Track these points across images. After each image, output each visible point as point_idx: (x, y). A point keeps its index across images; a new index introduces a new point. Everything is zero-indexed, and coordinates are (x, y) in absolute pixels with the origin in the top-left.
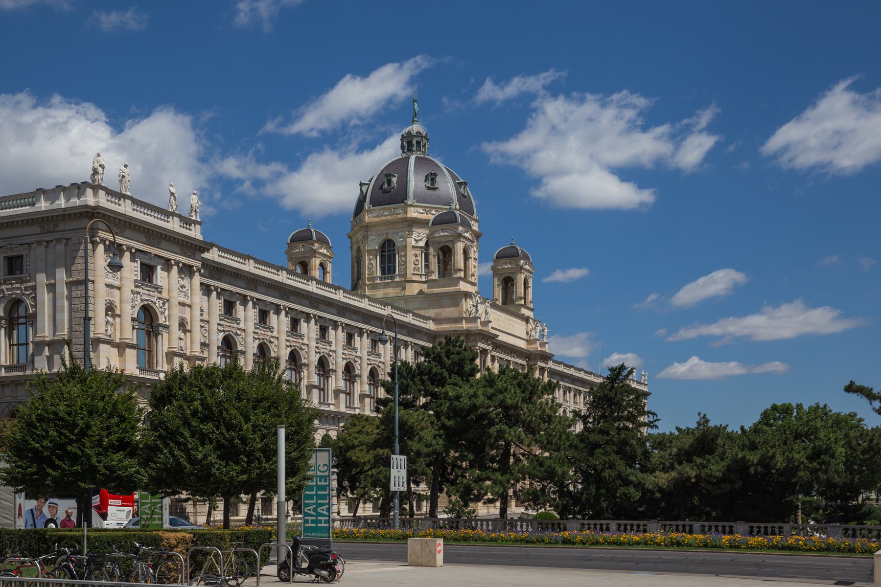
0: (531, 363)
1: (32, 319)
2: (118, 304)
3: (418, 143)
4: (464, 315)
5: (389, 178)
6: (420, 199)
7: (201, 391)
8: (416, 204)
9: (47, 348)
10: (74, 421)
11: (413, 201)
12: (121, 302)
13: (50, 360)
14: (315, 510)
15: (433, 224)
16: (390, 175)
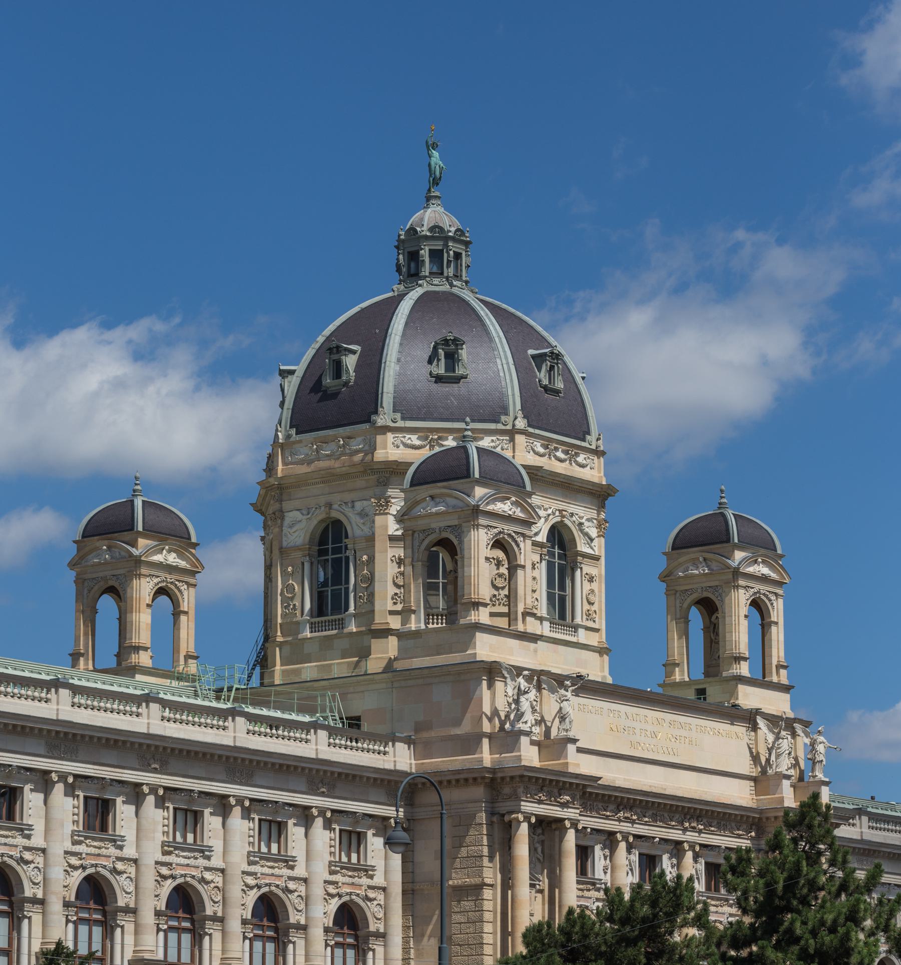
3: (436, 255)
5: (335, 357)
8: (401, 424)
11: (392, 415)
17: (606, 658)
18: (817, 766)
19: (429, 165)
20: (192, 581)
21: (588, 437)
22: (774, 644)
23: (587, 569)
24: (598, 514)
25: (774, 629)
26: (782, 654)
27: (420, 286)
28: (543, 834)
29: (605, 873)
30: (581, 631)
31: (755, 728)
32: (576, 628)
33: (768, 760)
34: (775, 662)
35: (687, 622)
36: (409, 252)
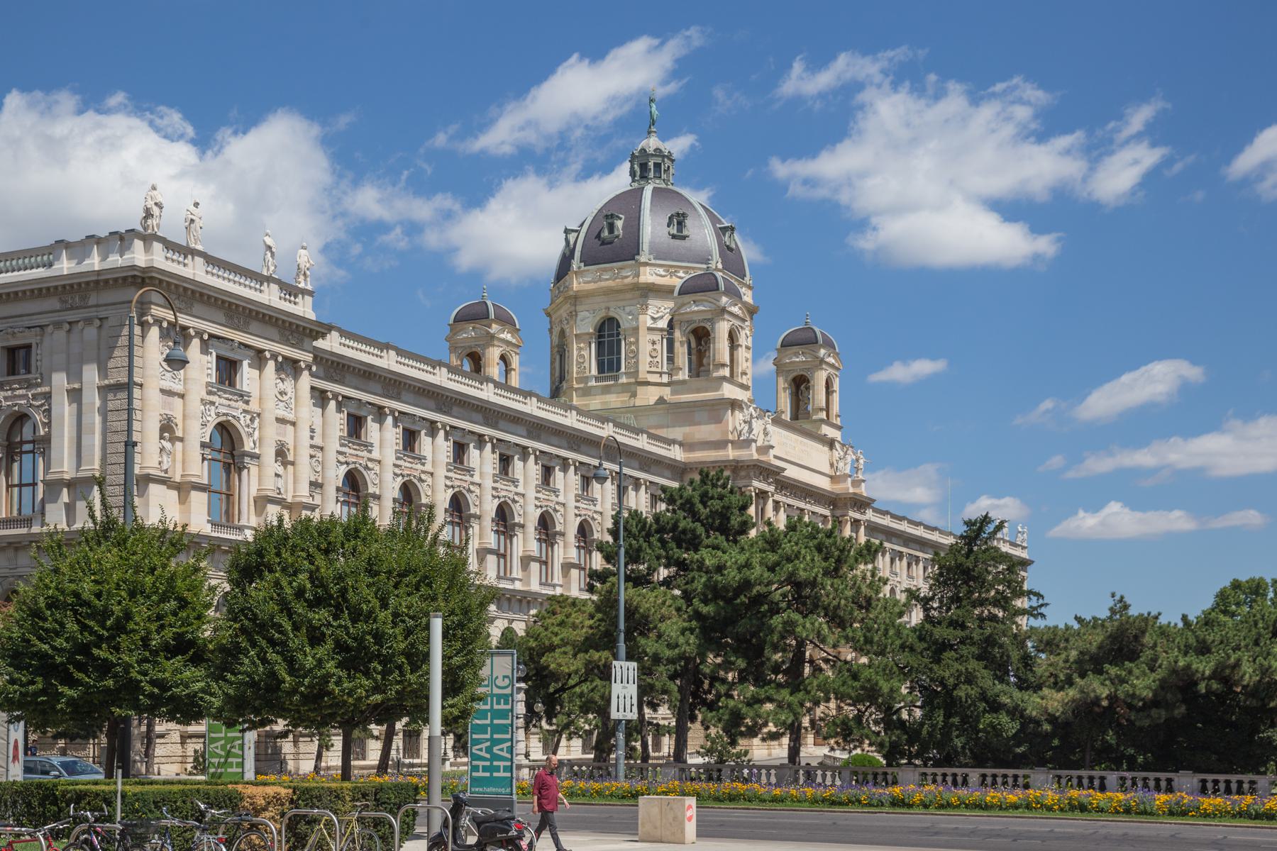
0: (838, 513)
1: (43, 445)
2: (179, 421)
3: (657, 166)
4: (730, 437)
5: (610, 221)
7: (310, 558)
8: (653, 261)
9: (65, 490)
10: (106, 607)
11: (649, 256)
12: (184, 416)
13: (70, 509)
14: (489, 750)
15: (679, 294)
16: (612, 215)
20: (518, 351)
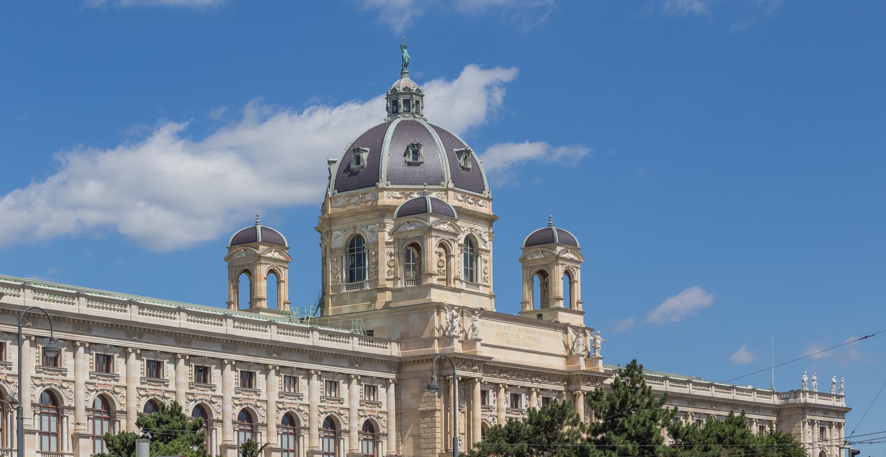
3: (406, 102)
6: (394, 179)
8: (390, 186)
11: (386, 182)
16: (358, 149)
17: (493, 300)
18: (597, 350)
19: (403, 56)
21: (484, 192)
22: (576, 292)
23: (483, 257)
24: (489, 230)
25: (576, 284)
26: (580, 296)
27: (399, 118)
28: (465, 385)
29: (494, 403)
30: (481, 287)
31: (566, 332)
32: (478, 286)
33: (573, 348)
34: (576, 301)
35: (533, 281)
36: (393, 101)
